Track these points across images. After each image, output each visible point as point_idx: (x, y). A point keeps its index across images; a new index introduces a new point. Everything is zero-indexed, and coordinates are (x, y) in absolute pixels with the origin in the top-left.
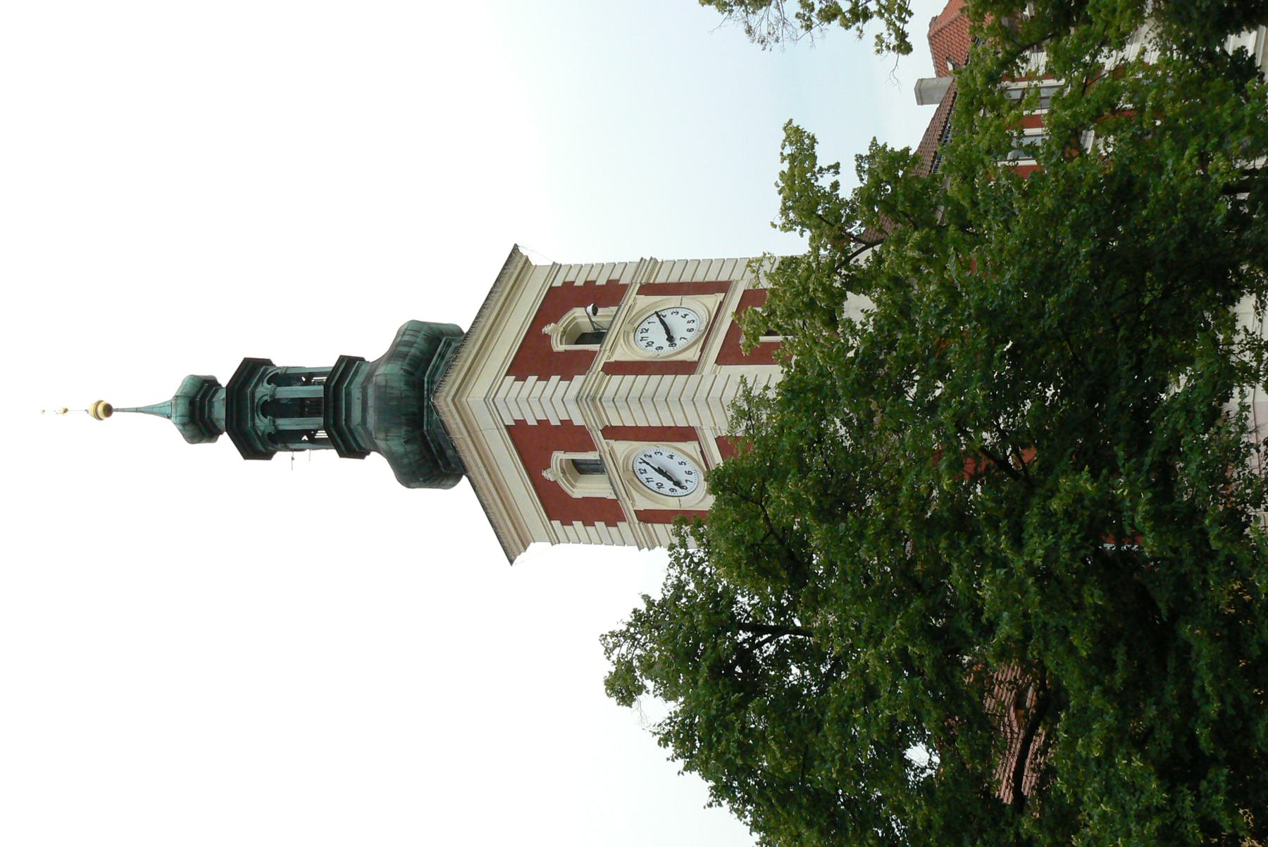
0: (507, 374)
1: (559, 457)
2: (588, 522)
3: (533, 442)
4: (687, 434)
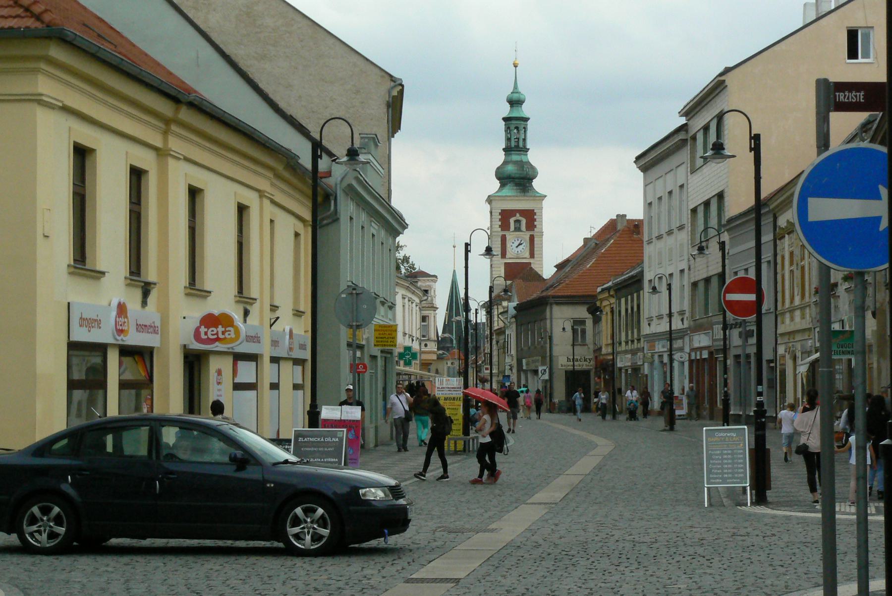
1: (524, 222)
2: (500, 220)
4: (532, 255)
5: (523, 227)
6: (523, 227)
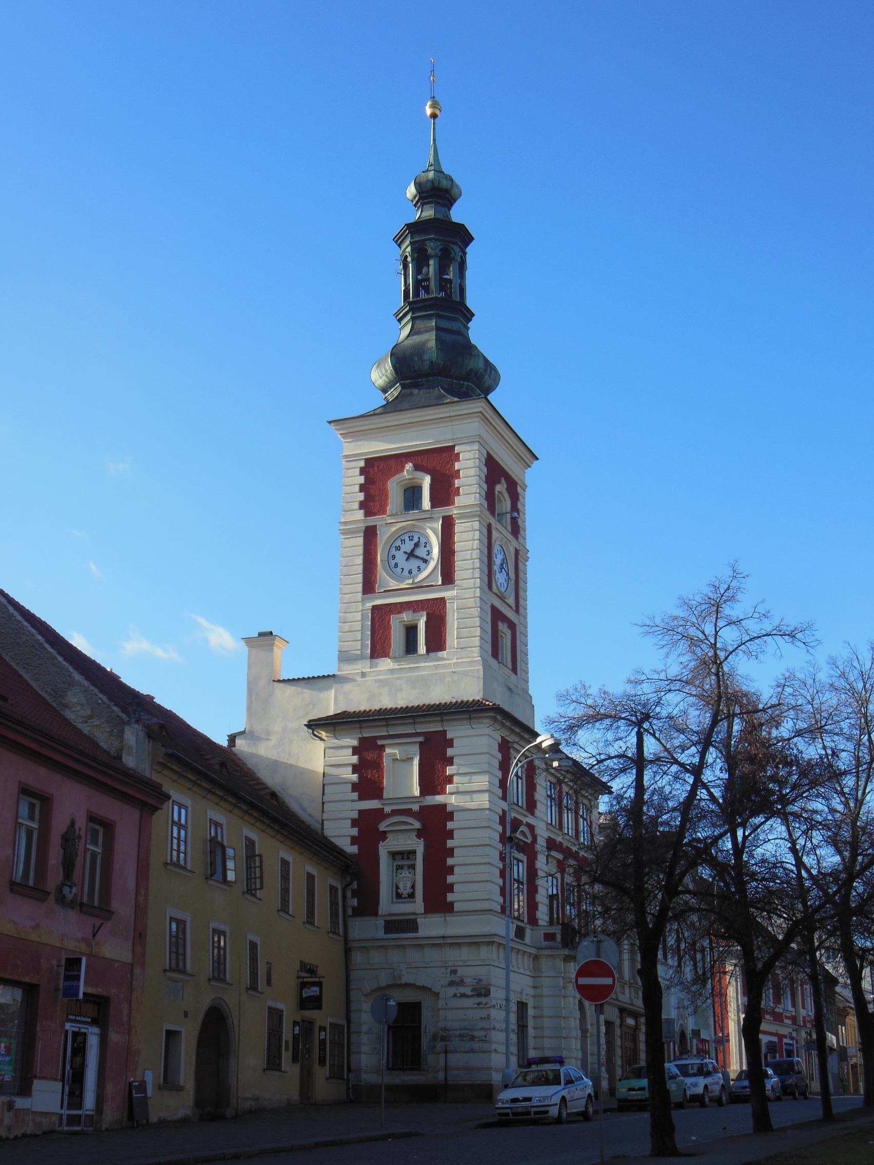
0: (488, 453)
1: (426, 481)
2: (362, 488)
3: (439, 464)
5: (426, 503)
6: (426, 503)
